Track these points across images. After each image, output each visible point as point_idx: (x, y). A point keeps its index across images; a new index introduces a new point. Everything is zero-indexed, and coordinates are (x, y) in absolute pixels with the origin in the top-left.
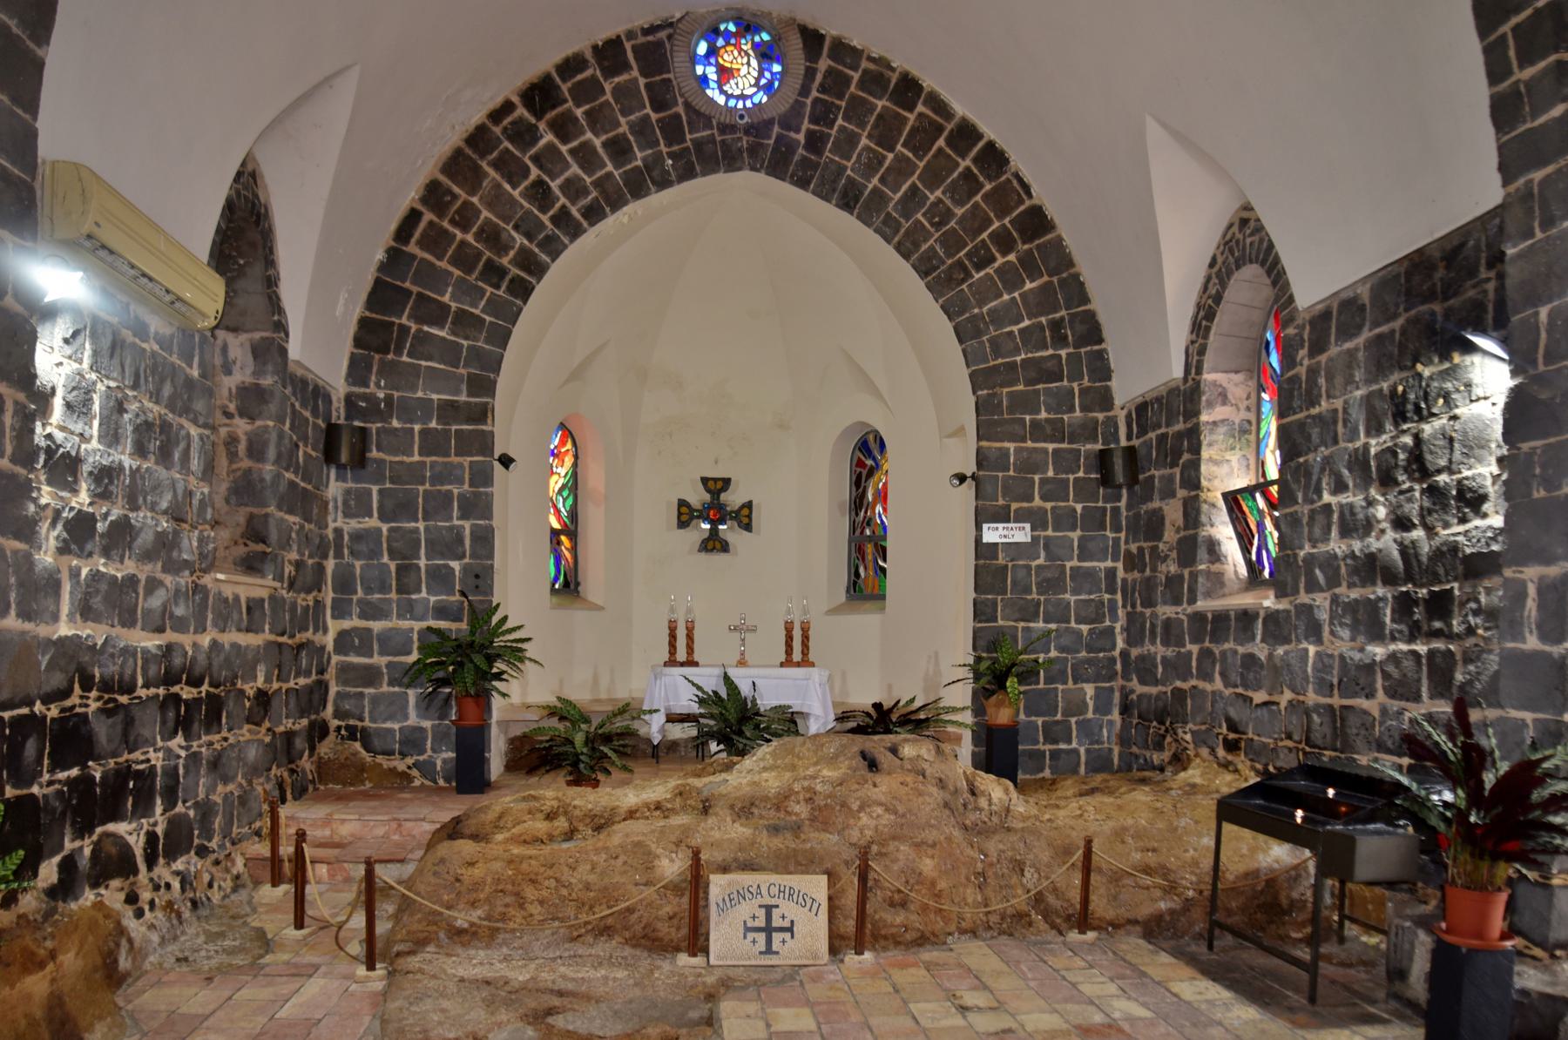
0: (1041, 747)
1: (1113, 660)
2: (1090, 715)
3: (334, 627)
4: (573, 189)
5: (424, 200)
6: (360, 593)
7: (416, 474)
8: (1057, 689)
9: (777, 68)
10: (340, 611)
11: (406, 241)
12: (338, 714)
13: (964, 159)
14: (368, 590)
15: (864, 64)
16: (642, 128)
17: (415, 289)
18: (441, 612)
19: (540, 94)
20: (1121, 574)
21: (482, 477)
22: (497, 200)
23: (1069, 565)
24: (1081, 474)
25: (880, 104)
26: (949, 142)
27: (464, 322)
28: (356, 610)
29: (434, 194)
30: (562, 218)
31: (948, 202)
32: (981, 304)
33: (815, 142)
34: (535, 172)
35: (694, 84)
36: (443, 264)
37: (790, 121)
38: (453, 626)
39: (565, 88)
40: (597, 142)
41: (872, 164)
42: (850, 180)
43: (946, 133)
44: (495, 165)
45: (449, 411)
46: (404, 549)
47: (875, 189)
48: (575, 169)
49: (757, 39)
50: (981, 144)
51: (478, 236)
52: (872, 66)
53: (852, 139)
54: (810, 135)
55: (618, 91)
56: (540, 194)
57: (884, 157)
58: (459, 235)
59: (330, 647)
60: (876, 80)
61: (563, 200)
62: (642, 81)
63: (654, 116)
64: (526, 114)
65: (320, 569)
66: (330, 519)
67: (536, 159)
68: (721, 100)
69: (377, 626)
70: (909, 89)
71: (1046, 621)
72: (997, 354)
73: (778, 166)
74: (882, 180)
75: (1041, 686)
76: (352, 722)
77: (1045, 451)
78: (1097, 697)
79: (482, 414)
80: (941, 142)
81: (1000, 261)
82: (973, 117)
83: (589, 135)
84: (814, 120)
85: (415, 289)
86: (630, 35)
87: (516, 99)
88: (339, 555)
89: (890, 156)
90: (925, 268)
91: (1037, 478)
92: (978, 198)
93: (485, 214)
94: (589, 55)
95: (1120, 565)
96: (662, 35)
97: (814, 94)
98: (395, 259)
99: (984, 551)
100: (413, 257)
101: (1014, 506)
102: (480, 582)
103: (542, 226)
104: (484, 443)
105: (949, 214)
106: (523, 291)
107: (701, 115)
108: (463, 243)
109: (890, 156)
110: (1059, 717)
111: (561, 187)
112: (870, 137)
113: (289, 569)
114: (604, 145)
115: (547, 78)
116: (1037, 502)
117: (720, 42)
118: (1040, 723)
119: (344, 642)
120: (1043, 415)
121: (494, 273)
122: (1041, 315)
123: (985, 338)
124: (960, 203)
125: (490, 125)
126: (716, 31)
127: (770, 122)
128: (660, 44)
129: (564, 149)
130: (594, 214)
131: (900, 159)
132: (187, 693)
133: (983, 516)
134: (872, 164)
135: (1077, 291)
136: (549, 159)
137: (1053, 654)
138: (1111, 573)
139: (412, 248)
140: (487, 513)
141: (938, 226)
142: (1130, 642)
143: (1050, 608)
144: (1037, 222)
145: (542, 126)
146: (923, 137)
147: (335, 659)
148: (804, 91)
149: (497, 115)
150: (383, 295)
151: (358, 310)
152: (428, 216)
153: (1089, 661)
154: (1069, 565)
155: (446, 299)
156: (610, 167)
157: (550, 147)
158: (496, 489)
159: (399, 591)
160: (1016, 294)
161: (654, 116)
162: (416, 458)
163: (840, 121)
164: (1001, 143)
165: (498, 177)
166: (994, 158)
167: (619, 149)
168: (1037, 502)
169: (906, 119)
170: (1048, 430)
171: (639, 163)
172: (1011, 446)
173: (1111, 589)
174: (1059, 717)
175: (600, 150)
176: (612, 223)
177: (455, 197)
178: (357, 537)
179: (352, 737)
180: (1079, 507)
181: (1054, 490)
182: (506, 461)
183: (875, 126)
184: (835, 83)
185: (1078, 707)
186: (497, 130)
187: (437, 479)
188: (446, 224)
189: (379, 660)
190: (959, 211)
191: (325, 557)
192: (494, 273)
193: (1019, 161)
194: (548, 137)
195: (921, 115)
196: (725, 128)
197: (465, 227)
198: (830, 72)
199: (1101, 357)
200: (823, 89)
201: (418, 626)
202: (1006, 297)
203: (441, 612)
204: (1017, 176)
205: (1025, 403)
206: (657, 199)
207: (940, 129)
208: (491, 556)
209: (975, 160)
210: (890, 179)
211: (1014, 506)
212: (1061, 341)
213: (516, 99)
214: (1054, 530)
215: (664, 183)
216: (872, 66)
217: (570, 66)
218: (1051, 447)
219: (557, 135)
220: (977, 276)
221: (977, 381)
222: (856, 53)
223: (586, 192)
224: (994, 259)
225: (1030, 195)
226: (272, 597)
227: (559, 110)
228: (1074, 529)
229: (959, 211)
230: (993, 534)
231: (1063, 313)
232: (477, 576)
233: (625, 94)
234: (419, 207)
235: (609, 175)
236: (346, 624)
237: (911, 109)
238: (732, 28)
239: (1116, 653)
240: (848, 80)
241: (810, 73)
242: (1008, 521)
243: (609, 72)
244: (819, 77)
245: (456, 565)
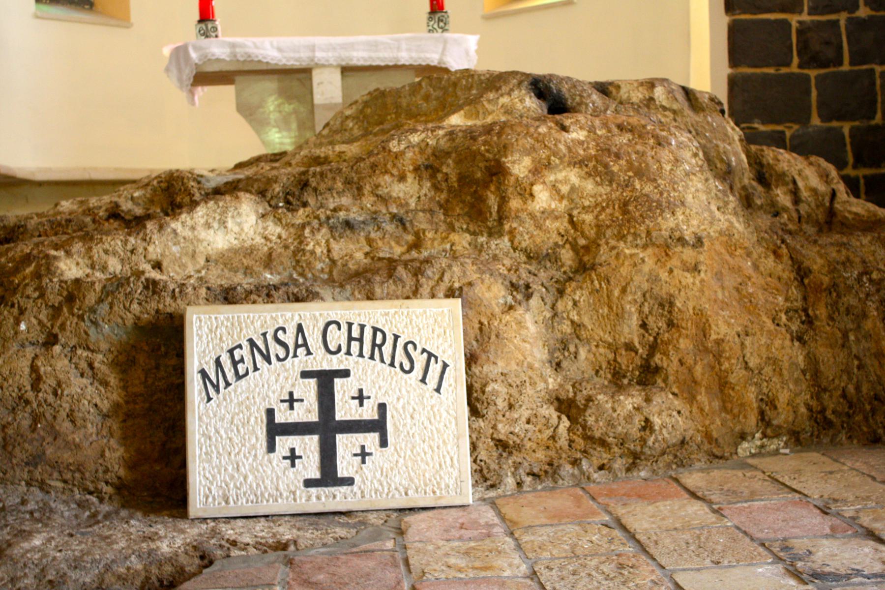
8: (872, 71)
75: (846, 67)
118: (846, 131)
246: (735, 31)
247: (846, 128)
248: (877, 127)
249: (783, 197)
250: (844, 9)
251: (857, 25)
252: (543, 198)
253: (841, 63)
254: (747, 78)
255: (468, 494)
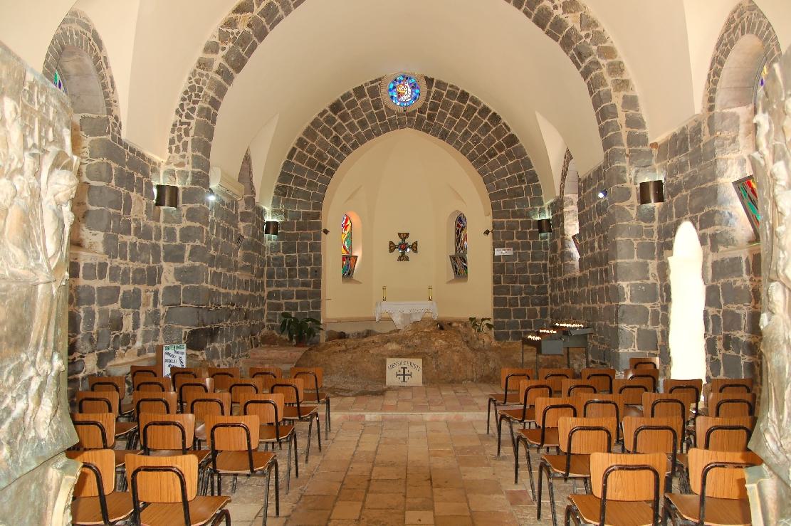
0: (520, 330)
1: (547, 298)
2: (539, 318)
3: (267, 290)
4: (348, 138)
5: (297, 144)
6: (276, 279)
7: (295, 237)
9: (417, 91)
10: (268, 286)
11: (291, 158)
12: (269, 320)
13: (484, 119)
14: (279, 277)
15: (448, 88)
16: (371, 116)
17: (295, 174)
18: (304, 284)
19: (336, 107)
20: (548, 265)
21: (318, 237)
22: (322, 143)
23: (528, 263)
24: (531, 229)
25: (454, 102)
26: (479, 113)
27: (311, 185)
28: (274, 284)
29: (301, 143)
30: (344, 148)
31: (479, 135)
32: (492, 170)
33: (431, 117)
34: (334, 133)
35: (388, 99)
36: (304, 166)
37: (421, 111)
38: (309, 288)
39: (344, 104)
40: (356, 122)
41: (451, 123)
42: (444, 130)
43: (478, 111)
44: (321, 131)
45: (306, 215)
46: (291, 264)
47: (452, 132)
48: (348, 131)
49: (410, 82)
50: (490, 114)
51: (316, 156)
52: (451, 89)
53: (444, 115)
54: (429, 115)
55: (362, 104)
56: (336, 140)
57: (455, 121)
58: (309, 156)
59: (265, 298)
60: (451, 94)
61: (344, 142)
62: (370, 100)
63: (375, 112)
64: (331, 113)
65: (263, 270)
66: (266, 252)
67: (335, 128)
68: (398, 104)
69: (282, 289)
70: (464, 96)
71: (520, 283)
72: (498, 188)
73: (418, 125)
74: (455, 129)
75: (519, 307)
76: (272, 323)
77: (518, 222)
78: (541, 312)
79: (318, 216)
80: (476, 114)
81: (499, 154)
82: (487, 105)
83: (353, 119)
84: (430, 109)
85: (295, 174)
86: (366, 84)
87: (327, 109)
88: (269, 265)
89: (458, 120)
90: (472, 158)
91: (515, 231)
92: (490, 133)
93: (318, 148)
94: (352, 92)
95: (548, 262)
96: (377, 83)
97: (430, 100)
98: (287, 165)
99: (496, 259)
100: (294, 164)
101: (507, 242)
102: (317, 273)
103: (337, 151)
104: (318, 226)
105: (480, 139)
106: (331, 173)
107: (391, 111)
108: (310, 158)
109: (458, 120)
110: (527, 319)
111: (344, 138)
112: (450, 114)
113: (255, 271)
114: (358, 122)
115: (338, 100)
116: (515, 240)
117: (398, 83)
119: (270, 295)
120: (516, 208)
121: (321, 168)
122: (515, 172)
123: (494, 182)
124: (484, 135)
125: (319, 118)
126: (396, 80)
127: (415, 111)
128: (376, 87)
129: (344, 125)
130: (355, 146)
131: (461, 120)
132: (231, 308)
133: (495, 246)
134: (451, 123)
135: (528, 164)
136: (339, 129)
137: (523, 295)
138: (545, 265)
139: (293, 161)
140: (319, 249)
141: (475, 144)
142: (552, 290)
143: (521, 279)
144: (512, 140)
145: (337, 117)
146: (471, 110)
147: (267, 301)
148: (427, 99)
149: (321, 114)
150: (284, 177)
151: (275, 183)
152: (299, 150)
153: (537, 298)
154: (528, 263)
155: (305, 177)
156: (360, 130)
157: (340, 124)
158: (322, 242)
159: (289, 278)
160: (505, 166)
161: (375, 112)
162: (295, 232)
163: (440, 109)
164: (498, 114)
165: (322, 135)
166: (495, 118)
167: (363, 124)
168: (515, 240)
169: (463, 107)
170: (518, 213)
171: (370, 128)
172: (505, 220)
173: (546, 272)
174: (527, 319)
175: (356, 124)
176: (361, 148)
177: (308, 143)
178: (275, 259)
179: (273, 329)
180: (531, 242)
181: (522, 235)
182: (326, 232)
183: (453, 109)
184: (438, 96)
185: (533, 314)
186: (322, 119)
187: (303, 238)
188: (305, 152)
189: (283, 301)
190: (483, 138)
191: (264, 266)
192: (321, 168)
193: (504, 120)
194: (339, 121)
195: (469, 105)
196: (398, 114)
197: (311, 152)
198: (436, 92)
199: (538, 186)
200: (434, 98)
201: (295, 289)
202: (501, 167)
203: (304, 284)
204: (504, 124)
205: (511, 205)
206: (376, 139)
207: (475, 109)
208: (320, 264)
209: (488, 120)
210: (458, 128)
211: (507, 242)
212: (523, 182)
213: (327, 109)
214: (522, 250)
215: (378, 134)
216: (451, 89)
217: (345, 97)
218: (520, 220)
219: (342, 120)
220: (490, 161)
221: (492, 197)
222: (445, 85)
223: (352, 139)
224: (497, 154)
225: (509, 131)
226: (251, 280)
227: (342, 111)
228: (530, 250)
229: (483, 138)
230: (498, 252)
231: (523, 171)
232: (316, 271)
233: (364, 104)
234: (295, 147)
235: (360, 133)
236: (271, 289)
237: (465, 103)
238: (402, 79)
239: (548, 295)
240: (442, 94)
241: (429, 93)
242: (504, 247)
243: (359, 98)
244: (432, 94)
245: (309, 268)
246: (495, 298)
247: (519, 320)
248: (526, 321)
249: (481, 342)
250: (519, 294)
251: (522, 299)
252: (436, 344)
253: (518, 306)
254: (497, 310)
255: (421, 385)
